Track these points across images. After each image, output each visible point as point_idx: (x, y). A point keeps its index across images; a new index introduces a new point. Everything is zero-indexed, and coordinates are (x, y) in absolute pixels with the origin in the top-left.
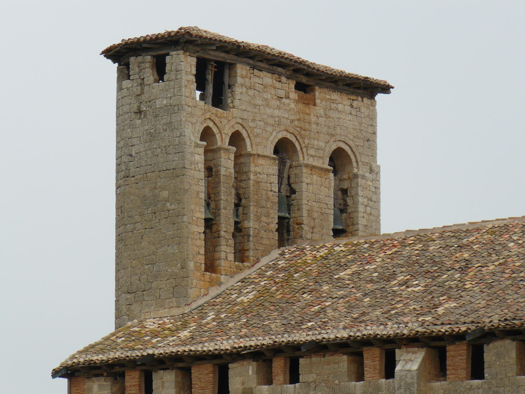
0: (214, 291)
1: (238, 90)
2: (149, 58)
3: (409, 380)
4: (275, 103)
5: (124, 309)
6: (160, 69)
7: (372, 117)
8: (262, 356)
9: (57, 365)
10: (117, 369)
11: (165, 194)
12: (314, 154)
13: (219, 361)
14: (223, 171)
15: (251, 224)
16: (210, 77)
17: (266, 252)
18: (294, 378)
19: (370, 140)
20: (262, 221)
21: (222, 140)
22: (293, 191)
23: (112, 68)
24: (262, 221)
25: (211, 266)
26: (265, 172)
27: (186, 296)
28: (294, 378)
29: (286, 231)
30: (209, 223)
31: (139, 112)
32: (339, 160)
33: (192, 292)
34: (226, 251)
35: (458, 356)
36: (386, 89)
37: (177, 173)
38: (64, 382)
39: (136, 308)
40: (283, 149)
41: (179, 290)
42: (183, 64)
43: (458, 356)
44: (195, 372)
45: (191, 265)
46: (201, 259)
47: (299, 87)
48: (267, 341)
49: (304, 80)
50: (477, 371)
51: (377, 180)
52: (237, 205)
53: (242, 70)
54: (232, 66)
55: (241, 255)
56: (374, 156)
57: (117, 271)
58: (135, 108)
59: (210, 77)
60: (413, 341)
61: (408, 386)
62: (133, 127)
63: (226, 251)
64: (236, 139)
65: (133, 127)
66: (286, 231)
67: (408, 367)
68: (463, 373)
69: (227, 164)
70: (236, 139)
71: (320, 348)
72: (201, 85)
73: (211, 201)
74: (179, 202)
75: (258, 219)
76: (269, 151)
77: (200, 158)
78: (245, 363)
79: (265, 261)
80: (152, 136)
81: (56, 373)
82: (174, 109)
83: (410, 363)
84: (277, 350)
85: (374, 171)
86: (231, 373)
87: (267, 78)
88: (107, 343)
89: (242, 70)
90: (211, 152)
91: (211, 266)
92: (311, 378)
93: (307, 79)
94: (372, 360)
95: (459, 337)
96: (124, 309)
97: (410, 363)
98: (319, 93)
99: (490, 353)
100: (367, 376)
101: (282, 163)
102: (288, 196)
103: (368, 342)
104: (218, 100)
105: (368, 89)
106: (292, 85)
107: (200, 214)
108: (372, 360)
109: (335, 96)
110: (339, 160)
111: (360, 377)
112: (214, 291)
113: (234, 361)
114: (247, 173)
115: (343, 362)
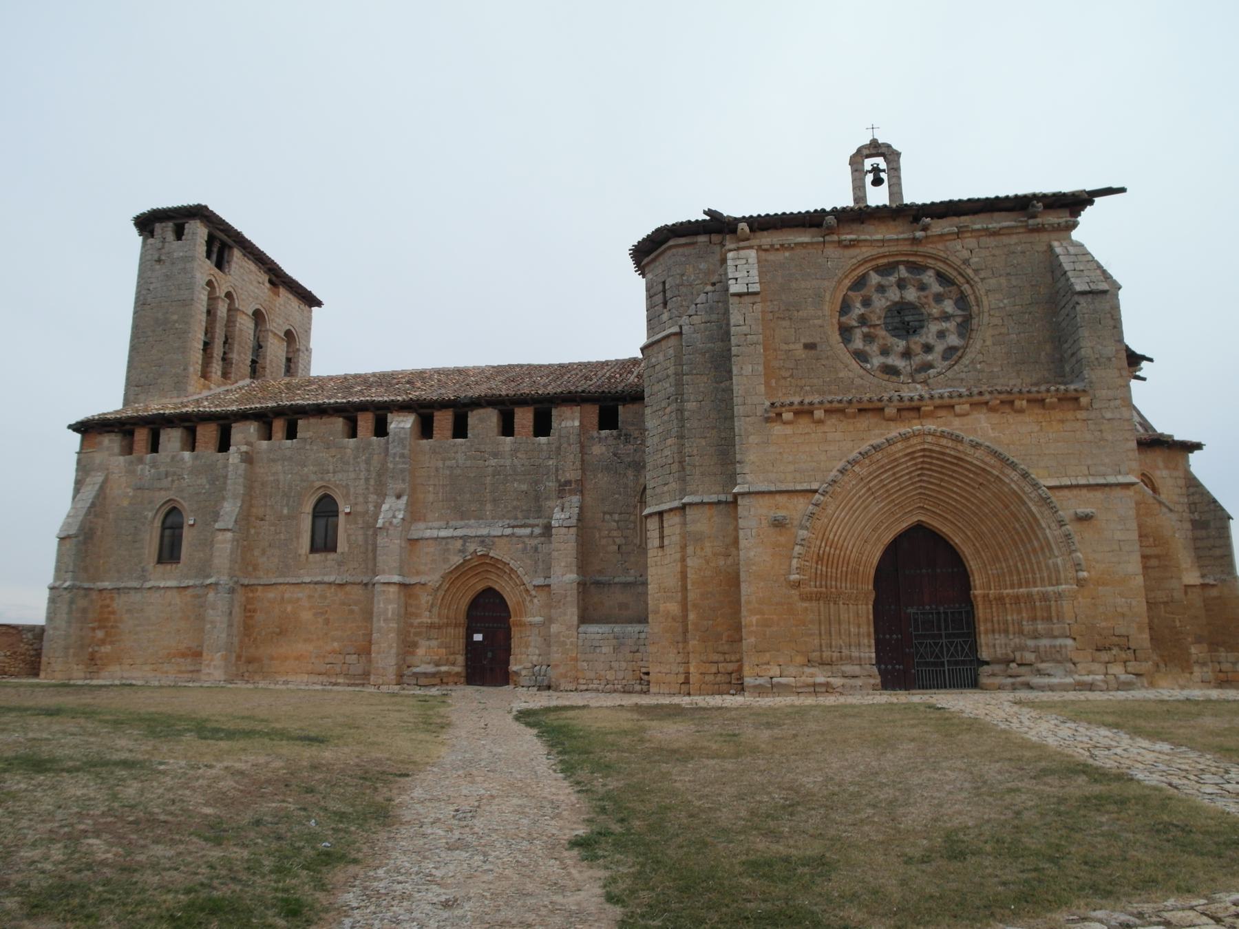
0: (205, 393)
1: (234, 265)
2: (171, 224)
3: (402, 436)
4: (255, 283)
5: (132, 398)
6: (179, 233)
7: (310, 318)
8: (264, 418)
9: (73, 422)
10: (128, 427)
11: (175, 317)
12: (277, 325)
13: (221, 422)
14: (219, 313)
15: (234, 356)
16: (215, 250)
17: (242, 378)
18: (291, 434)
19: (307, 331)
20: (242, 357)
21: (221, 292)
22: (260, 347)
23: (135, 240)
24: (242, 357)
25: (205, 375)
26: (245, 325)
27: (185, 390)
28: (291, 434)
29: (255, 369)
30: (207, 346)
31: (159, 261)
32: (289, 334)
33: (191, 389)
34: (216, 368)
35: (443, 420)
36: (318, 303)
37: (187, 303)
38: (77, 437)
39: (142, 397)
40: (258, 317)
41: (180, 385)
42: (198, 232)
43: (443, 420)
44: (200, 430)
45: (191, 369)
46: (199, 367)
47: (270, 282)
48: (271, 404)
49: (274, 279)
50: (460, 430)
51: (309, 356)
52: (225, 343)
53: (237, 254)
54: (231, 248)
55: (225, 375)
56: (309, 342)
57: (129, 371)
58: (156, 257)
59: (215, 250)
60: (404, 407)
61: (401, 441)
62: (153, 270)
63: (216, 368)
64: (229, 295)
65: (153, 270)
66: (255, 369)
67: (402, 425)
68: (449, 433)
69: (222, 309)
70: (229, 295)
71: (320, 411)
72: (209, 256)
73: (209, 331)
74: (187, 323)
75: (239, 354)
76: (250, 313)
77: (204, 297)
78: (248, 423)
79: (241, 383)
80: (168, 277)
81: (70, 427)
82: (189, 259)
83: (402, 424)
84: (279, 412)
85: (308, 350)
86: (233, 431)
87: (252, 266)
88: (117, 412)
89: (237, 254)
90: (212, 299)
91: (205, 375)
92: (309, 434)
93: (278, 278)
94: (365, 422)
95: (443, 405)
96: (132, 398)
97: (402, 424)
98: (282, 290)
99: (473, 418)
100: (360, 434)
101: (256, 325)
102: (259, 347)
103: (363, 407)
104: (220, 265)
105: (311, 300)
106: (267, 278)
107: (201, 336)
108: (365, 422)
109: (291, 296)
110: (289, 336)
111: (353, 434)
112: (205, 393)
113: (235, 421)
114: (234, 322)
115: (339, 423)
